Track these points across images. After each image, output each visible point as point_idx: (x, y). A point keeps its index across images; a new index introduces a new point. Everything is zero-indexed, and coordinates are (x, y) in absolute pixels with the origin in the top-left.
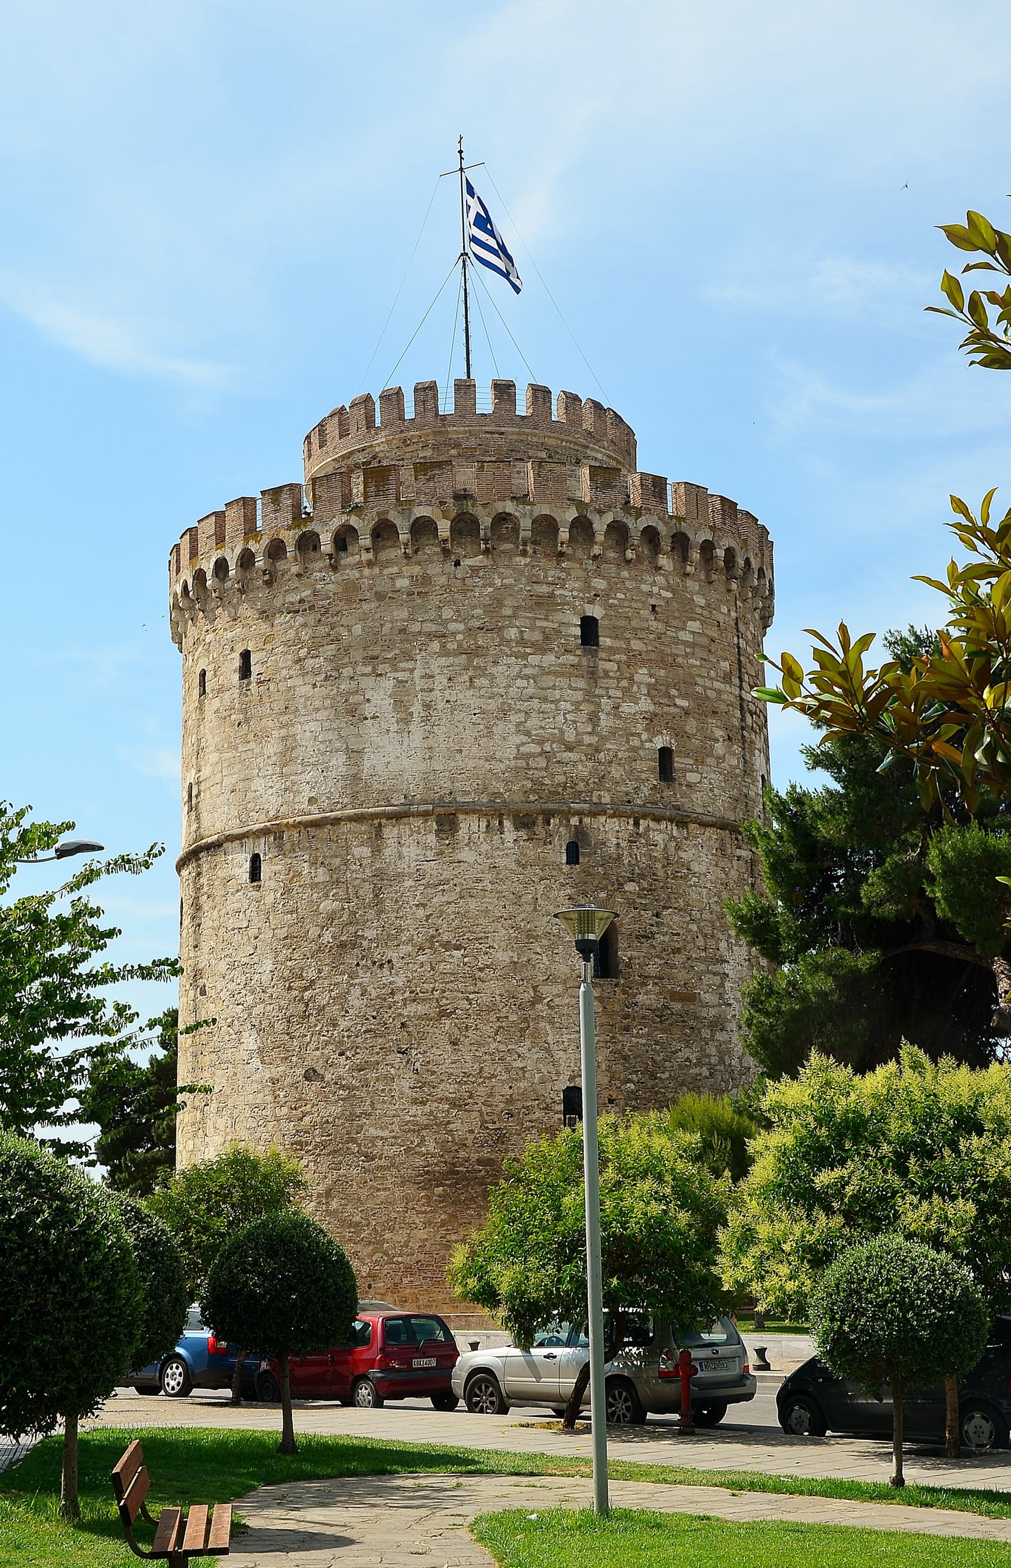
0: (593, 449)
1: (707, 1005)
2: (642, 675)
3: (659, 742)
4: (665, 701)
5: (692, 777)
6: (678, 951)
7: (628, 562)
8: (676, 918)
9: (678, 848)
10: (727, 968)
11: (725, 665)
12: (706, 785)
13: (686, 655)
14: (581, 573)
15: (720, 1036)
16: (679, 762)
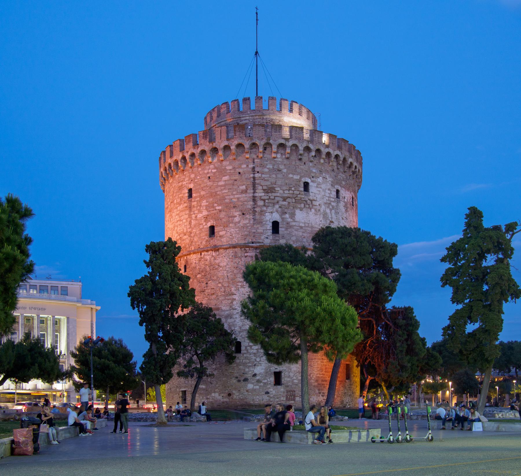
0: (243, 117)
1: (224, 311)
2: (204, 203)
3: (209, 224)
4: (212, 209)
5: (221, 233)
6: (214, 294)
7: (200, 165)
8: (213, 283)
9: (215, 259)
10: (234, 297)
11: (244, 187)
12: (229, 234)
13: (222, 190)
14: (188, 175)
15: (229, 320)
16: (216, 229)
